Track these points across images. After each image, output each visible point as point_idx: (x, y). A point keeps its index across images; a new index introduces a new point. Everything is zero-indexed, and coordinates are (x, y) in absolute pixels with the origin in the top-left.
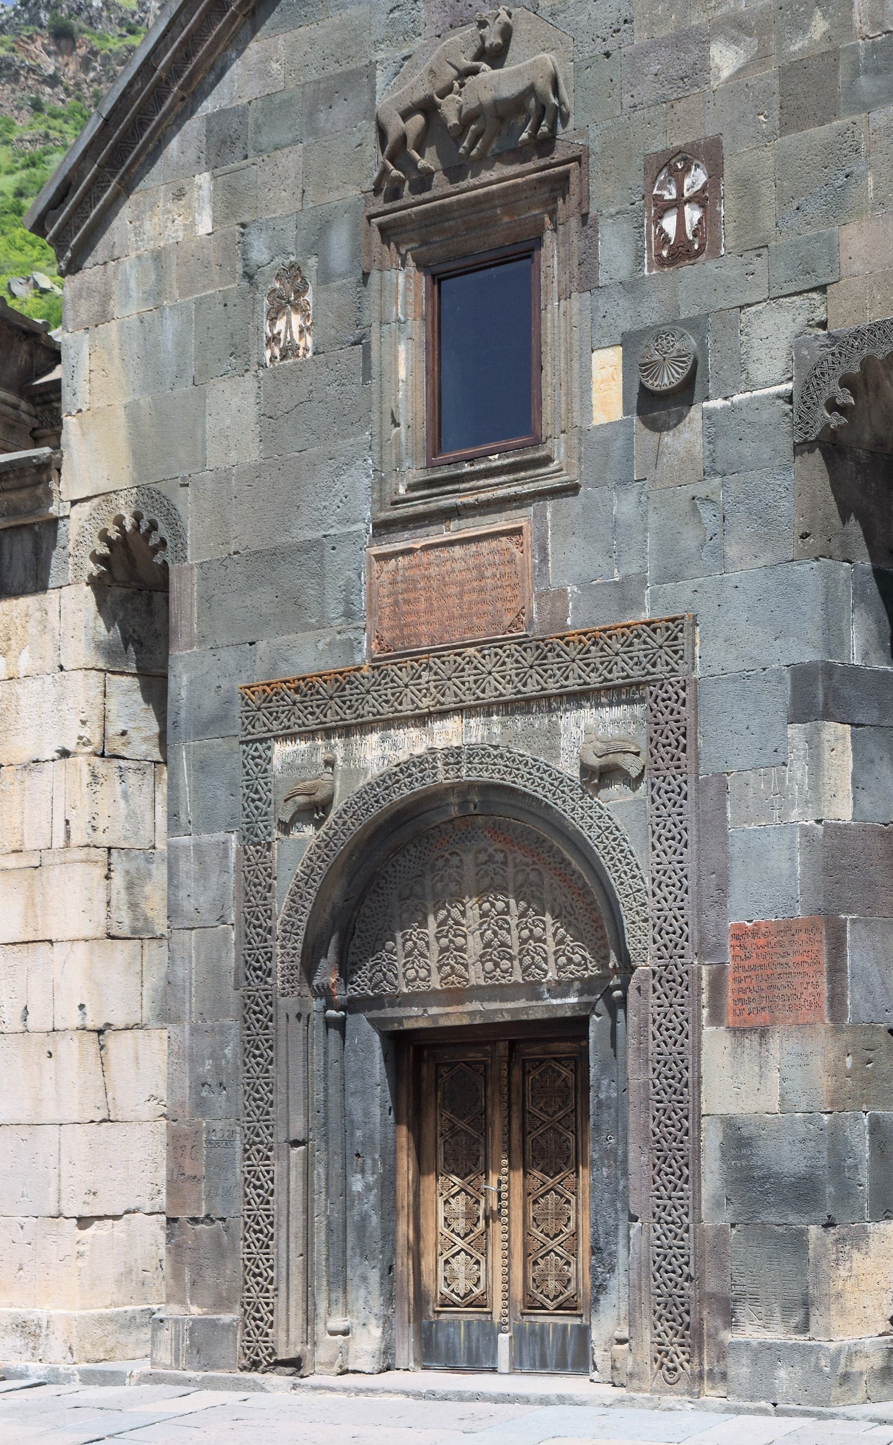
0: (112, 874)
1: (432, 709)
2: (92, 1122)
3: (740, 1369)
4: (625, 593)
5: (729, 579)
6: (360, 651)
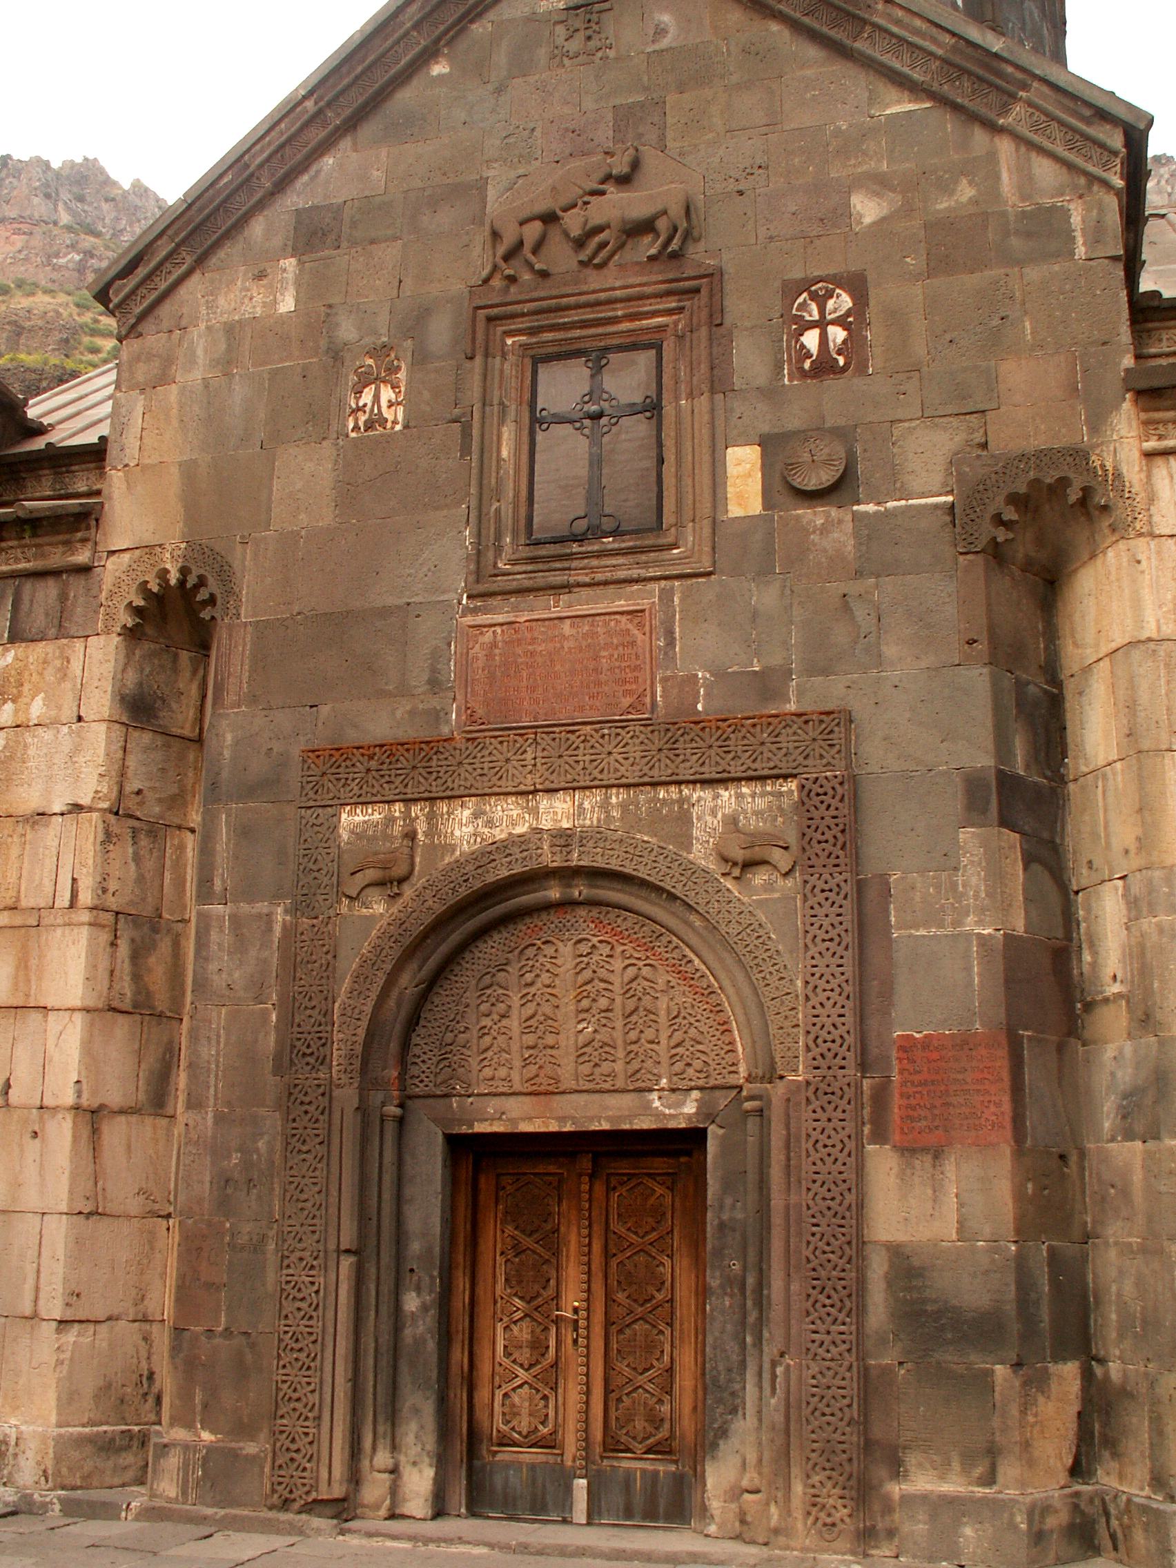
0: (119, 941)
1: (538, 787)
2: (80, 1213)
3: (917, 1527)
4: (768, 684)
5: (887, 678)
6: (448, 721)
